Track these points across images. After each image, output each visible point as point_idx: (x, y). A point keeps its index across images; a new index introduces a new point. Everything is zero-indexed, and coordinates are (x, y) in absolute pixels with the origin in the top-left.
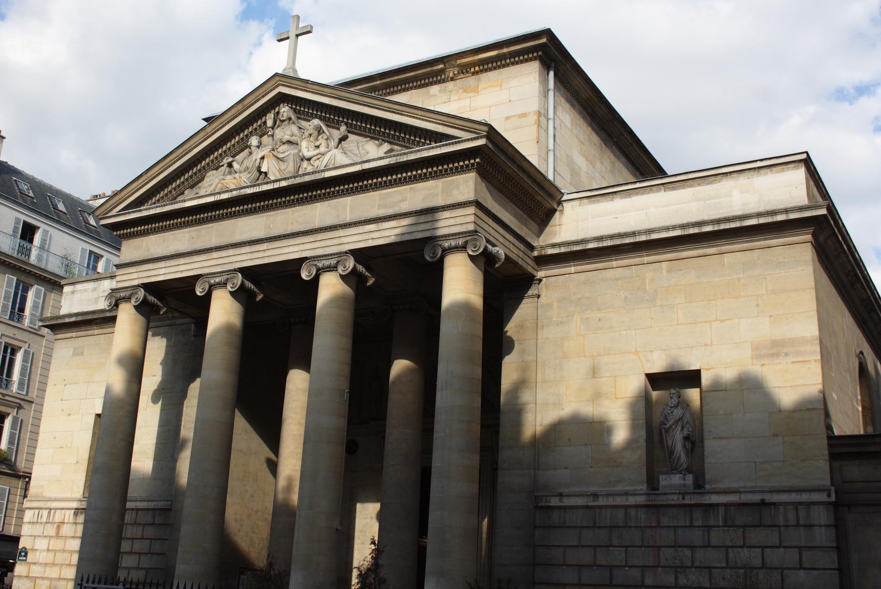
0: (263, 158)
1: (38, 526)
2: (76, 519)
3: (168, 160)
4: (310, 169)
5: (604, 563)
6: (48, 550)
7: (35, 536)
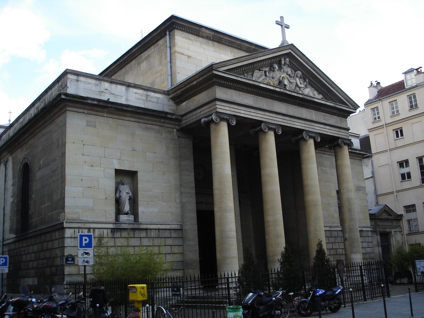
0: (283, 77)
2: (113, 235)
4: (300, 92)
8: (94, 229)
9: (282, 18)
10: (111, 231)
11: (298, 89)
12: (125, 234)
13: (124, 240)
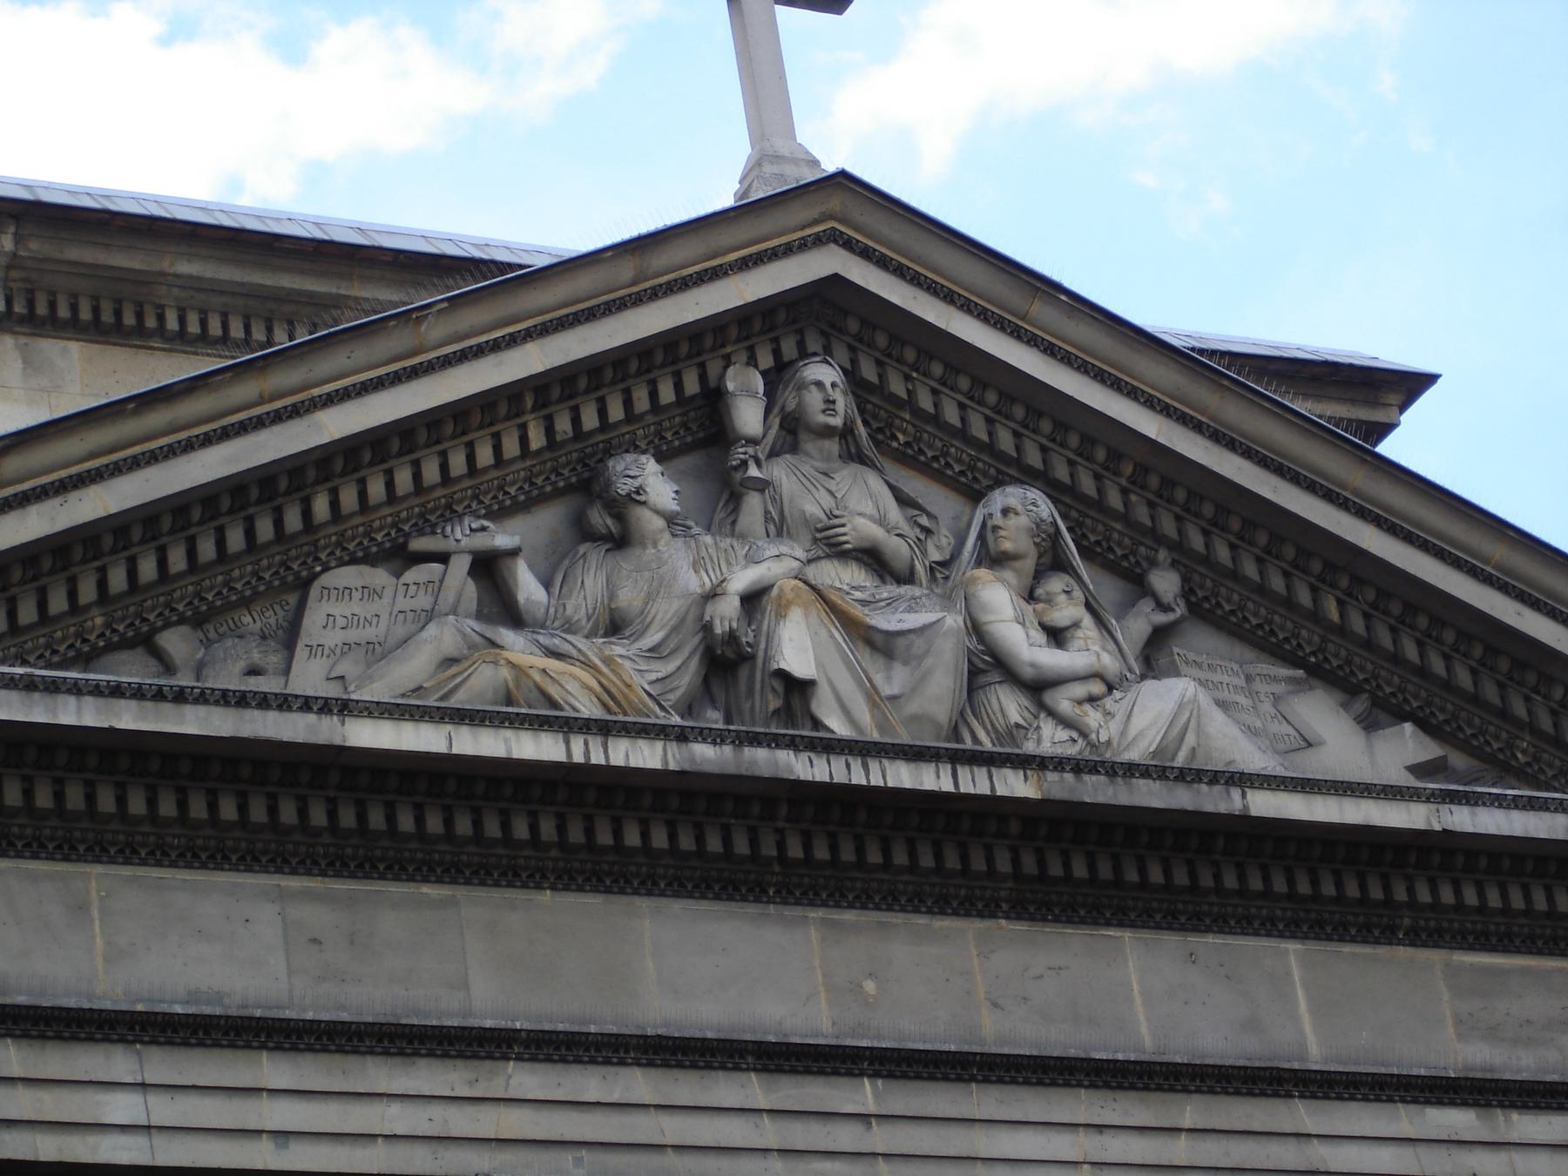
0: (753, 600)
3: (158, 418)
4: (1050, 739)
11: (1010, 705)
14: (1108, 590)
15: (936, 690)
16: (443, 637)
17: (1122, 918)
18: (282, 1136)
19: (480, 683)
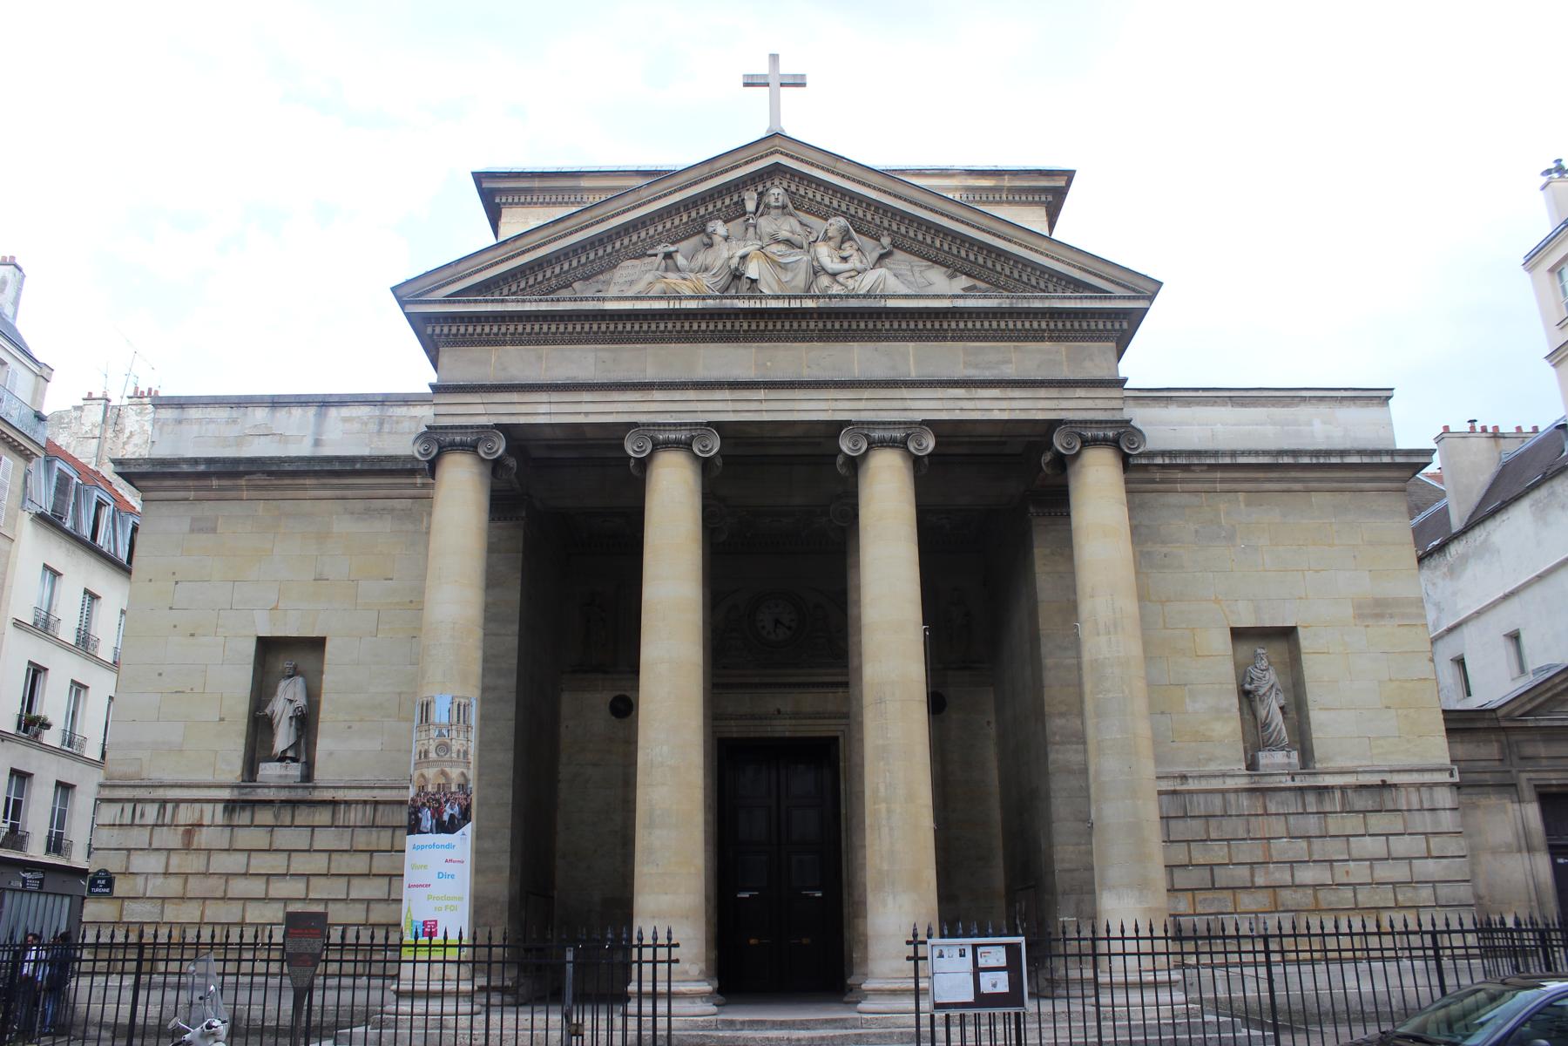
0: (744, 258)
1: (136, 831)
2: (230, 818)
3: (561, 226)
4: (836, 289)
5: (1202, 861)
6: (166, 874)
7: (129, 850)
8: (177, 802)
9: (774, 58)
10: (225, 809)
11: (824, 281)
12: (264, 816)
13: (262, 833)
14: (867, 242)
15: (799, 280)
16: (649, 277)
17: (854, 339)
18: (587, 414)
19: (657, 289)
